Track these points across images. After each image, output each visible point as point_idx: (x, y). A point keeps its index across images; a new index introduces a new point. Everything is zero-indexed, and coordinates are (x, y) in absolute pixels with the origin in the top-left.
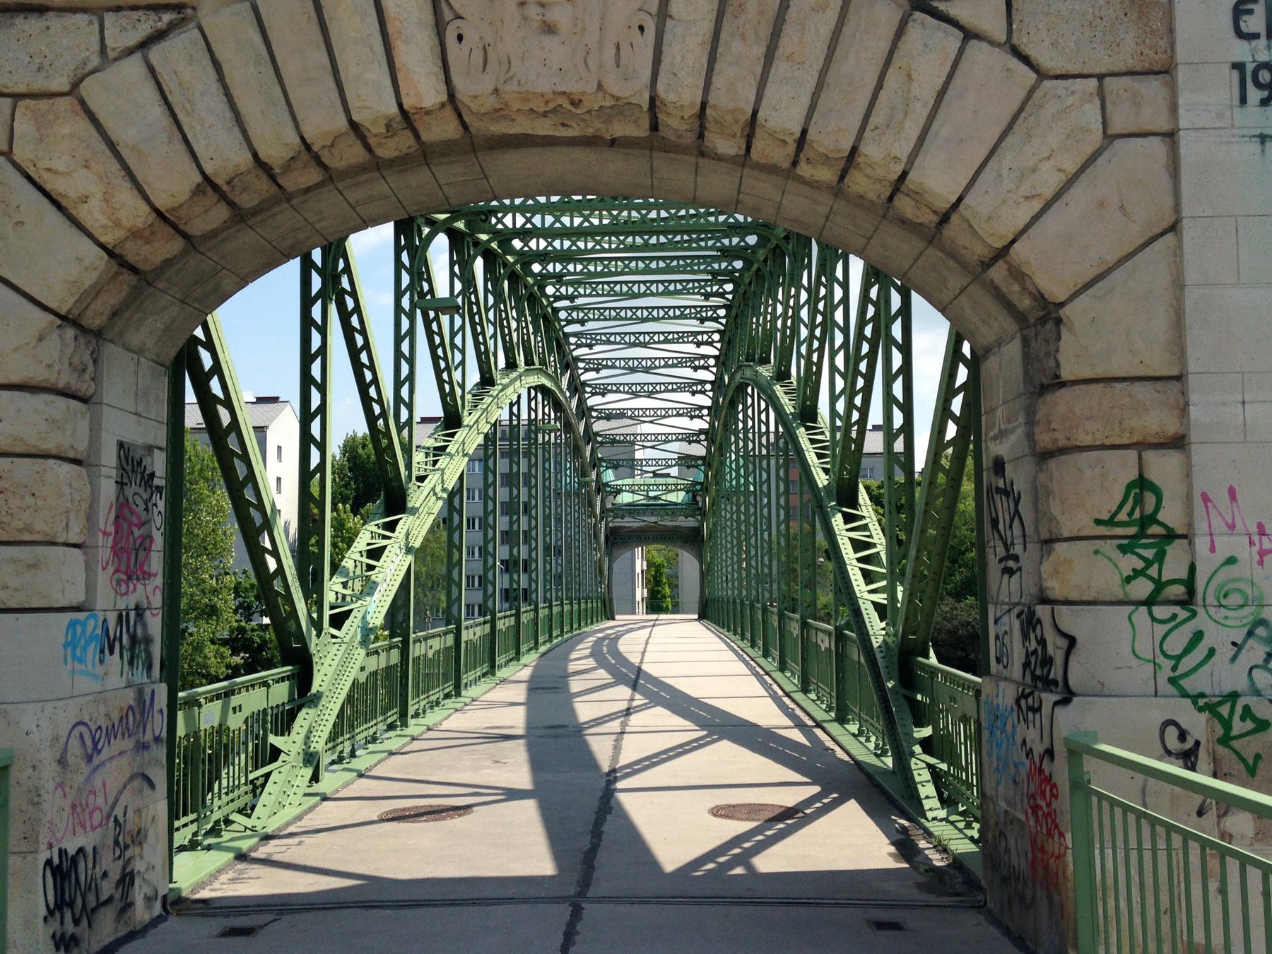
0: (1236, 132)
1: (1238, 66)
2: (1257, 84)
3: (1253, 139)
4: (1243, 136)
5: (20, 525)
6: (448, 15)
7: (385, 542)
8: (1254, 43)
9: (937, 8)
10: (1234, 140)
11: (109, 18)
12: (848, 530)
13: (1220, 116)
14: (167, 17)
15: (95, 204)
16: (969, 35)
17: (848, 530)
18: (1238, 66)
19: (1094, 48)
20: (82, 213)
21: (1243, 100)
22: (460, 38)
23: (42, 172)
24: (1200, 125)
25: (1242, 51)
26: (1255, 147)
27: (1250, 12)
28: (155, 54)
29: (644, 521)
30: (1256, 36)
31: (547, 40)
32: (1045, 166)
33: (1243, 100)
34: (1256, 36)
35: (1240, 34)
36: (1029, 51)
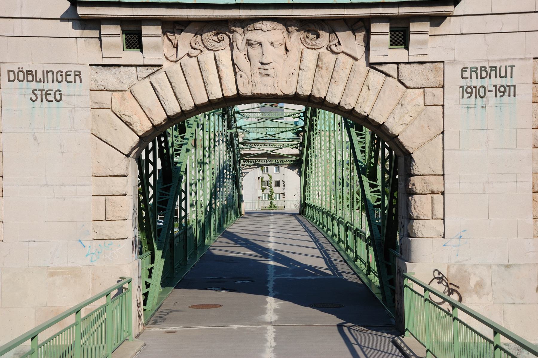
0: (460, 106)
1: (462, 87)
2: (467, 93)
3: (465, 108)
4: (462, 107)
5: (118, 215)
6: (237, 70)
7: (167, 197)
8: (467, 80)
9: (377, 68)
10: (460, 108)
11: (139, 68)
12: (371, 192)
13: (456, 101)
14: (156, 69)
15: (138, 125)
16: (387, 75)
17: (371, 192)
18: (462, 87)
19: (422, 81)
20: (134, 127)
21: (463, 98)
22: (241, 77)
23: (122, 115)
24: (450, 104)
25: (463, 83)
26: (466, 109)
27: (466, 71)
28: (153, 78)
29: (262, 150)
30: (467, 78)
31: (266, 78)
32: (407, 115)
33: (463, 98)
34: (467, 78)
35: (463, 78)
36: (403, 81)
